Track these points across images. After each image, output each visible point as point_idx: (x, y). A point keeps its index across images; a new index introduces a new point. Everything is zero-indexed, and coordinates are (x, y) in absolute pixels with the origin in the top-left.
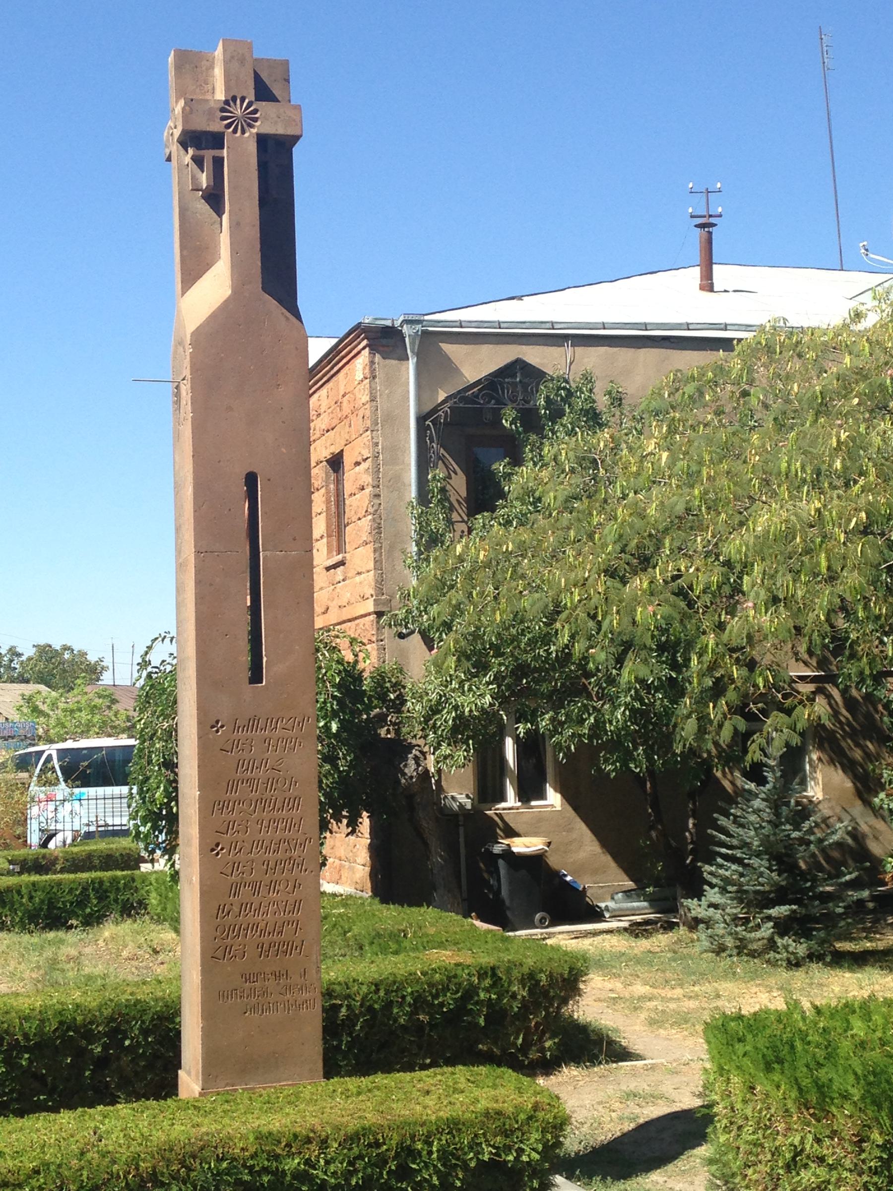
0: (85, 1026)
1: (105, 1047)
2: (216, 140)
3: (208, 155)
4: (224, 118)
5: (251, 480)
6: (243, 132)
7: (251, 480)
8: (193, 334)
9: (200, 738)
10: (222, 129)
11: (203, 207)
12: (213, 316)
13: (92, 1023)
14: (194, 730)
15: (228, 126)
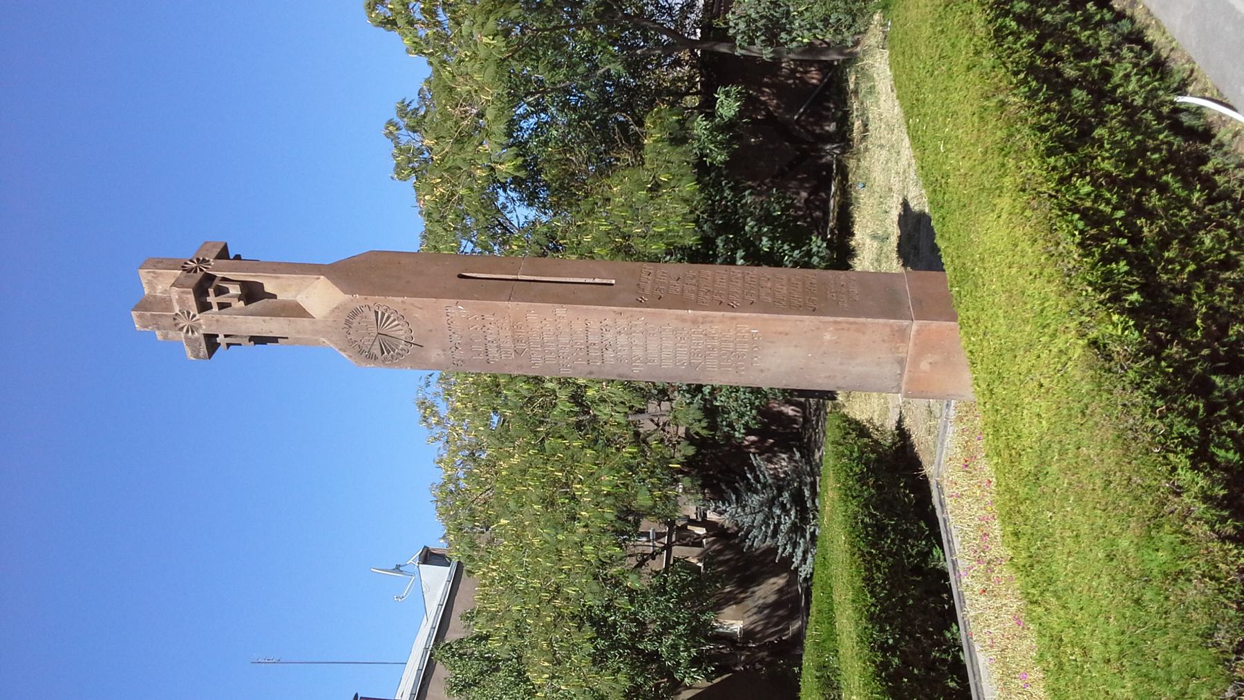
0: (877, 666)
1: (894, 655)
2: (209, 278)
3: (216, 282)
4: (196, 272)
5: (461, 276)
6: (210, 265)
7: (461, 276)
8: (345, 293)
9: (648, 307)
10: (203, 273)
11: (253, 306)
12: (336, 284)
13: (874, 662)
14: (642, 317)
15: (201, 270)
